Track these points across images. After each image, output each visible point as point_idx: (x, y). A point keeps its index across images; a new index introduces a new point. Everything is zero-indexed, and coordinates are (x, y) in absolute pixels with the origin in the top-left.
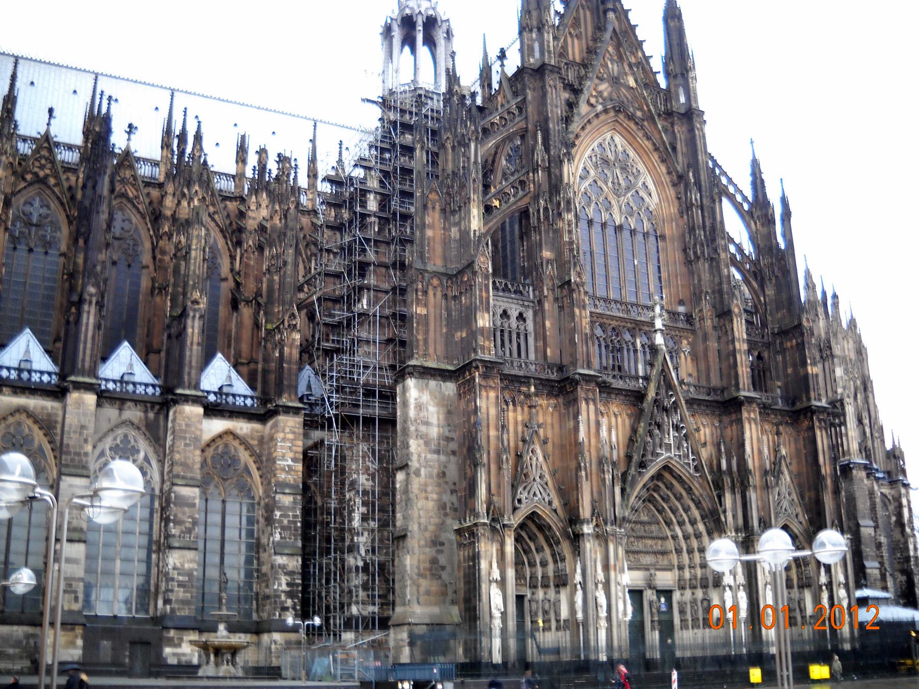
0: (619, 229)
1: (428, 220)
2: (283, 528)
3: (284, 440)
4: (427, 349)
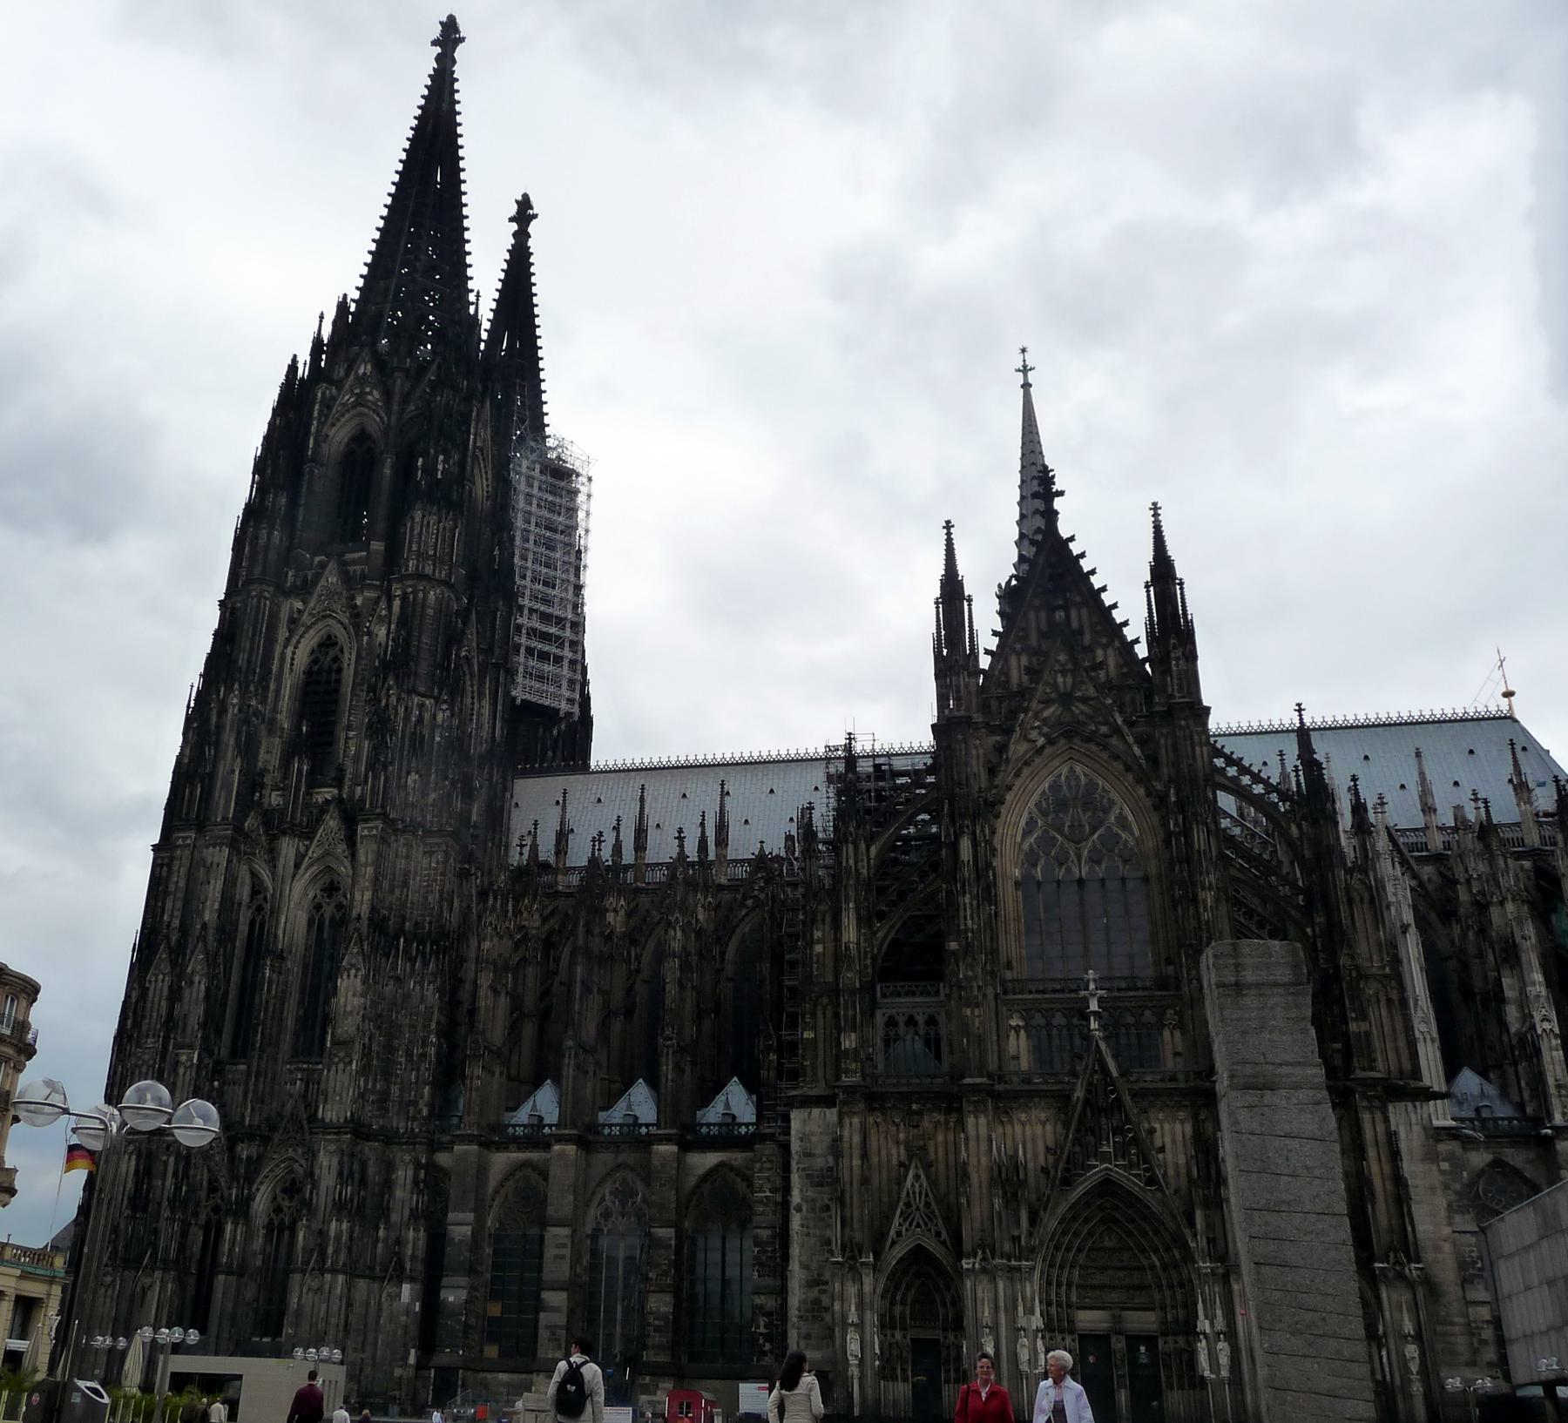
0: (1081, 882)
1: (817, 934)
2: (761, 1265)
3: (761, 1170)
4: (815, 1074)
